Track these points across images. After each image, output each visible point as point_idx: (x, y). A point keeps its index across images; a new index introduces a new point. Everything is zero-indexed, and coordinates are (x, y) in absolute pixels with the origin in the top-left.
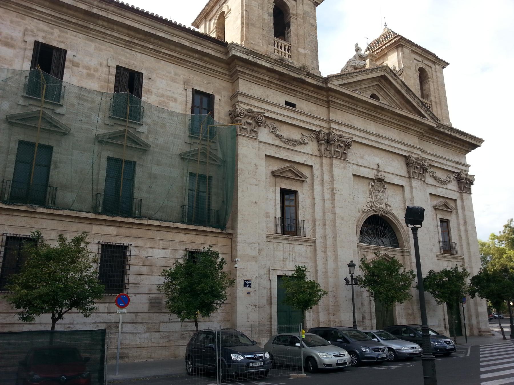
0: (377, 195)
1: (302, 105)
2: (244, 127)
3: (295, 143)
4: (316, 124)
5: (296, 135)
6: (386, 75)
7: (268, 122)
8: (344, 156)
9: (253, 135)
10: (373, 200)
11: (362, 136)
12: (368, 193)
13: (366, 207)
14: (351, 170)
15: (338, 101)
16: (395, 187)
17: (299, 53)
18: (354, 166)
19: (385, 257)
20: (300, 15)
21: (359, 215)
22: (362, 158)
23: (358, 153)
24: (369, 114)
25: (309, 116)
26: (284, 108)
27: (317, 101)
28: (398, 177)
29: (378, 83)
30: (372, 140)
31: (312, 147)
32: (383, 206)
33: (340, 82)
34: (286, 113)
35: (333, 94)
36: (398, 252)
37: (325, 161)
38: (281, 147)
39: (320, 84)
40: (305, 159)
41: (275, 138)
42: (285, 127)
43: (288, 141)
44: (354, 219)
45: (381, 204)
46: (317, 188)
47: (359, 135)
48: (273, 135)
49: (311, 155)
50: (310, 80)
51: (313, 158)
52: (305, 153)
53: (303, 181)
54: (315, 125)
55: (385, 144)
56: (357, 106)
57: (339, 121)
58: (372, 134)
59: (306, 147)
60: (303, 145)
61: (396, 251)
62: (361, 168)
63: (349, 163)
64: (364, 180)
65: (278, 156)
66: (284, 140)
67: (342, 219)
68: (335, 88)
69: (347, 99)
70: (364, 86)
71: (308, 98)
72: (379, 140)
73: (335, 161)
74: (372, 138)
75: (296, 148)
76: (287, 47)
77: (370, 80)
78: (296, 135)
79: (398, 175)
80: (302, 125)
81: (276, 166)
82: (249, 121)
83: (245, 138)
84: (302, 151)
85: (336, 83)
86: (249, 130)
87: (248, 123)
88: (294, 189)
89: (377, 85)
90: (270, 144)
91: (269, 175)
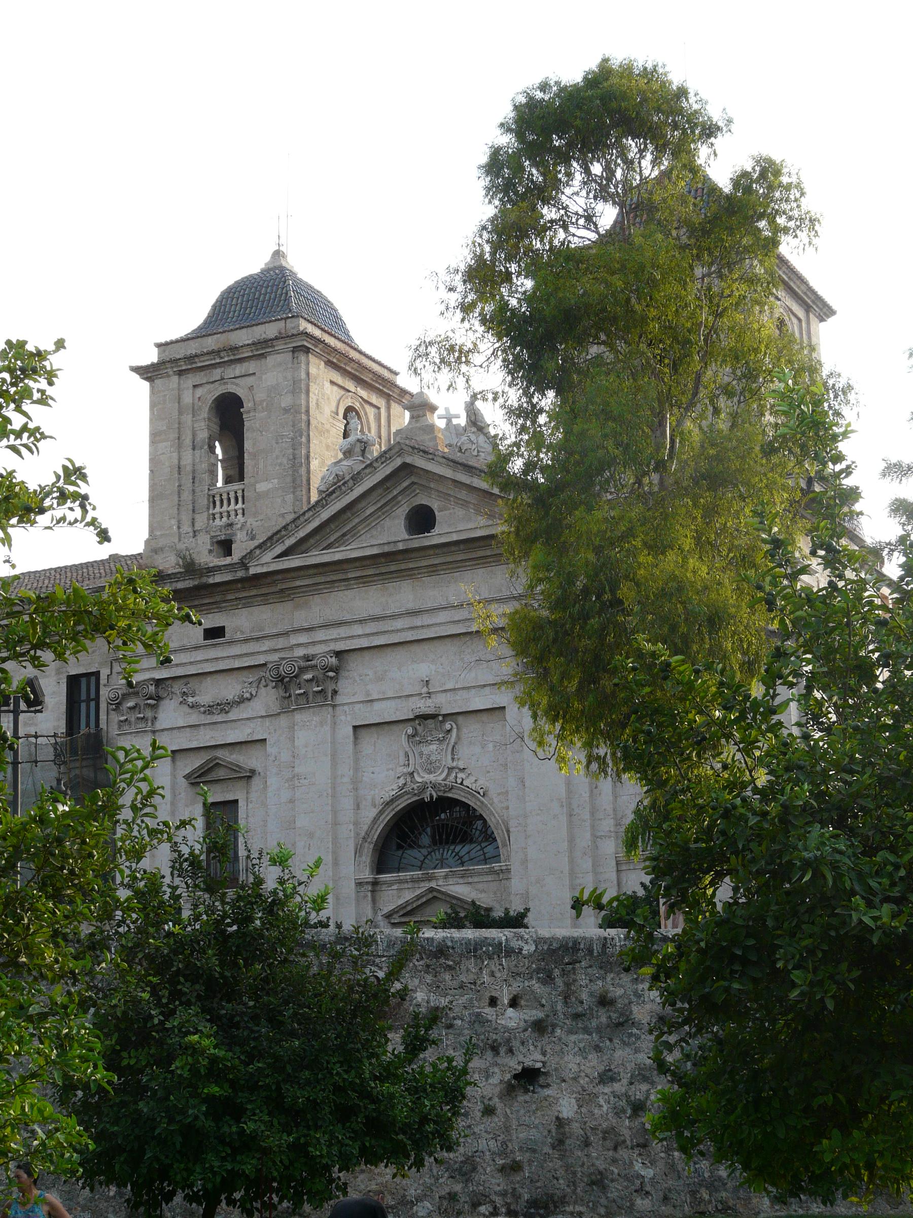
0: (421, 754)
1: (238, 621)
2: (122, 718)
3: (223, 707)
4: (264, 649)
5: (229, 689)
6: (408, 460)
7: (177, 688)
8: (319, 698)
9: (141, 725)
10: (411, 769)
11: (368, 631)
12: (402, 754)
13: (390, 790)
14: (349, 718)
15: (298, 583)
16: (484, 717)
17: (259, 496)
18: (358, 706)
19: (435, 894)
20: (262, 401)
21: (369, 814)
22: (380, 679)
23: (370, 673)
24: (382, 574)
25: (246, 641)
26: (197, 648)
27: (265, 599)
28: (488, 689)
29: (413, 479)
30: (400, 630)
31: (267, 699)
32: (438, 777)
33: (279, 549)
34: (200, 655)
35: (280, 577)
36: (487, 874)
37: (283, 721)
38: (199, 725)
39: (240, 574)
40: (249, 731)
41: (190, 711)
42: (209, 679)
43: (210, 710)
44: (351, 827)
45: (430, 773)
46: (273, 781)
47: (360, 633)
48: (185, 708)
49: (262, 717)
50: (218, 579)
51: (267, 722)
52: (248, 719)
53: (249, 777)
54: (261, 653)
55: (442, 623)
56: (345, 571)
57: (306, 625)
58: (393, 617)
59: (252, 703)
60: (247, 703)
61: (480, 874)
62: (377, 706)
63: (344, 704)
64: (395, 727)
65: (194, 744)
66: (202, 709)
67: (311, 835)
68: (265, 570)
69: (311, 571)
70: (368, 512)
71: (248, 603)
72: (418, 621)
73: (298, 717)
74: (399, 624)
75: (232, 716)
76: (240, 494)
77: (380, 491)
78: (229, 689)
79: (485, 686)
80: (237, 664)
81: (196, 762)
82: (131, 704)
83: (129, 737)
84: (245, 716)
85: (268, 556)
86: (133, 719)
87: (130, 708)
88: (230, 797)
89: (413, 483)
90: (179, 728)
91: (183, 783)
